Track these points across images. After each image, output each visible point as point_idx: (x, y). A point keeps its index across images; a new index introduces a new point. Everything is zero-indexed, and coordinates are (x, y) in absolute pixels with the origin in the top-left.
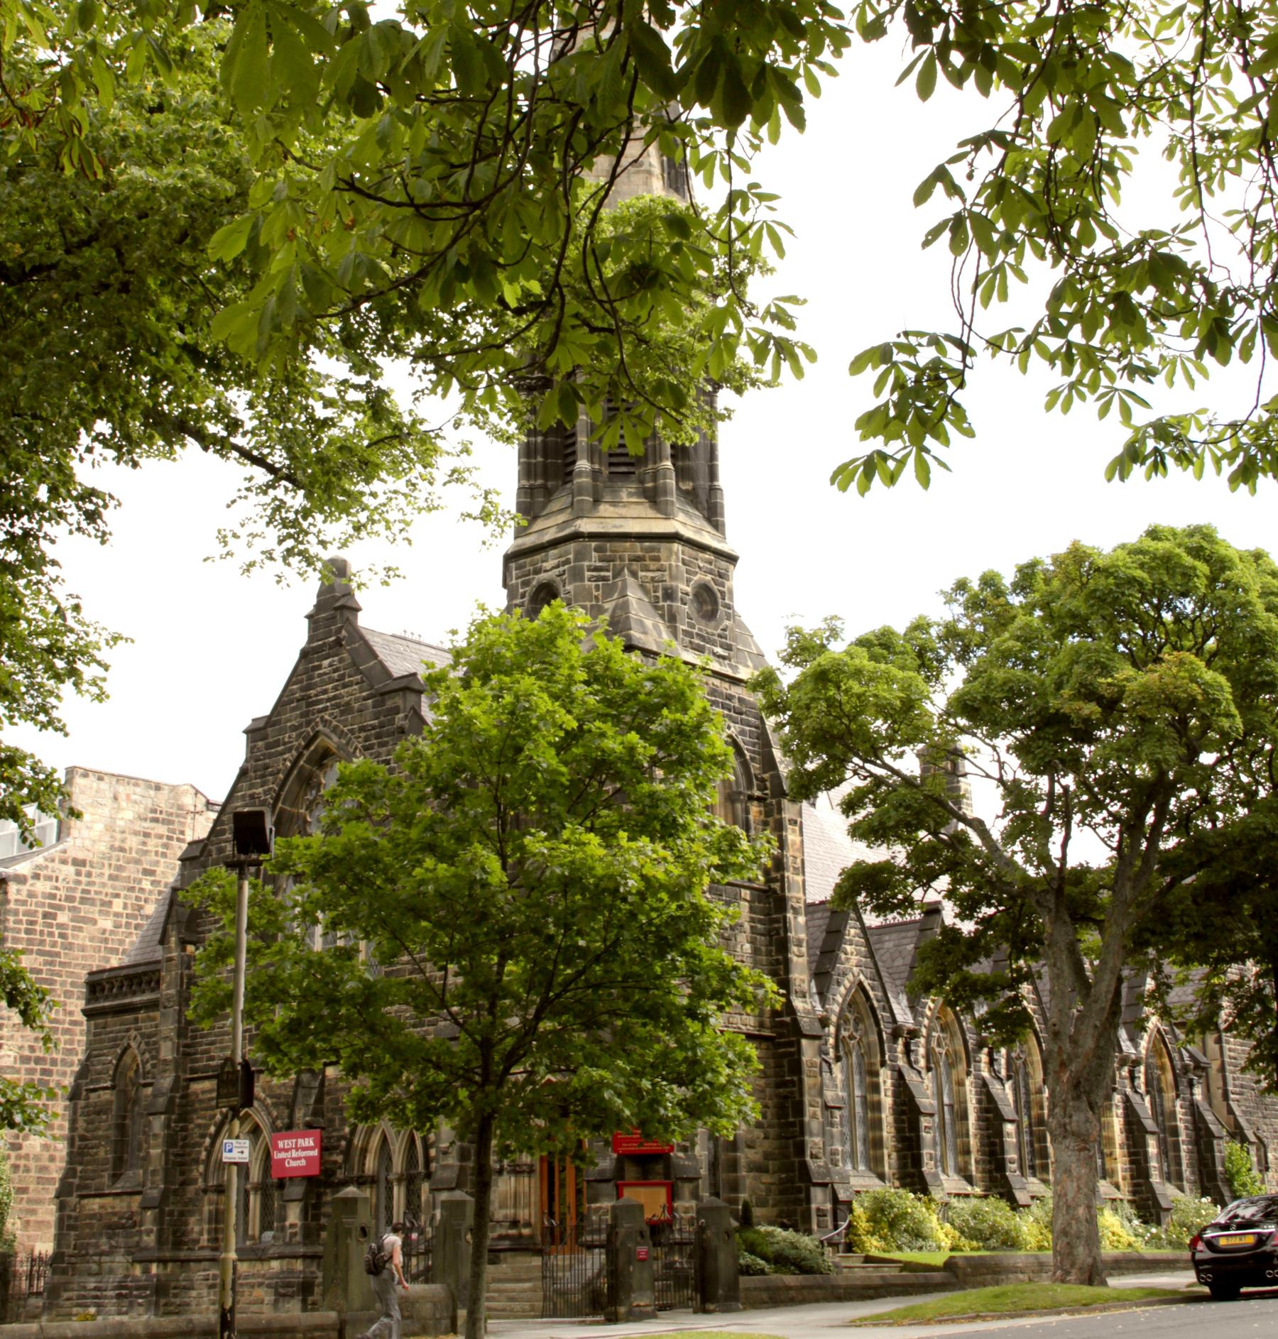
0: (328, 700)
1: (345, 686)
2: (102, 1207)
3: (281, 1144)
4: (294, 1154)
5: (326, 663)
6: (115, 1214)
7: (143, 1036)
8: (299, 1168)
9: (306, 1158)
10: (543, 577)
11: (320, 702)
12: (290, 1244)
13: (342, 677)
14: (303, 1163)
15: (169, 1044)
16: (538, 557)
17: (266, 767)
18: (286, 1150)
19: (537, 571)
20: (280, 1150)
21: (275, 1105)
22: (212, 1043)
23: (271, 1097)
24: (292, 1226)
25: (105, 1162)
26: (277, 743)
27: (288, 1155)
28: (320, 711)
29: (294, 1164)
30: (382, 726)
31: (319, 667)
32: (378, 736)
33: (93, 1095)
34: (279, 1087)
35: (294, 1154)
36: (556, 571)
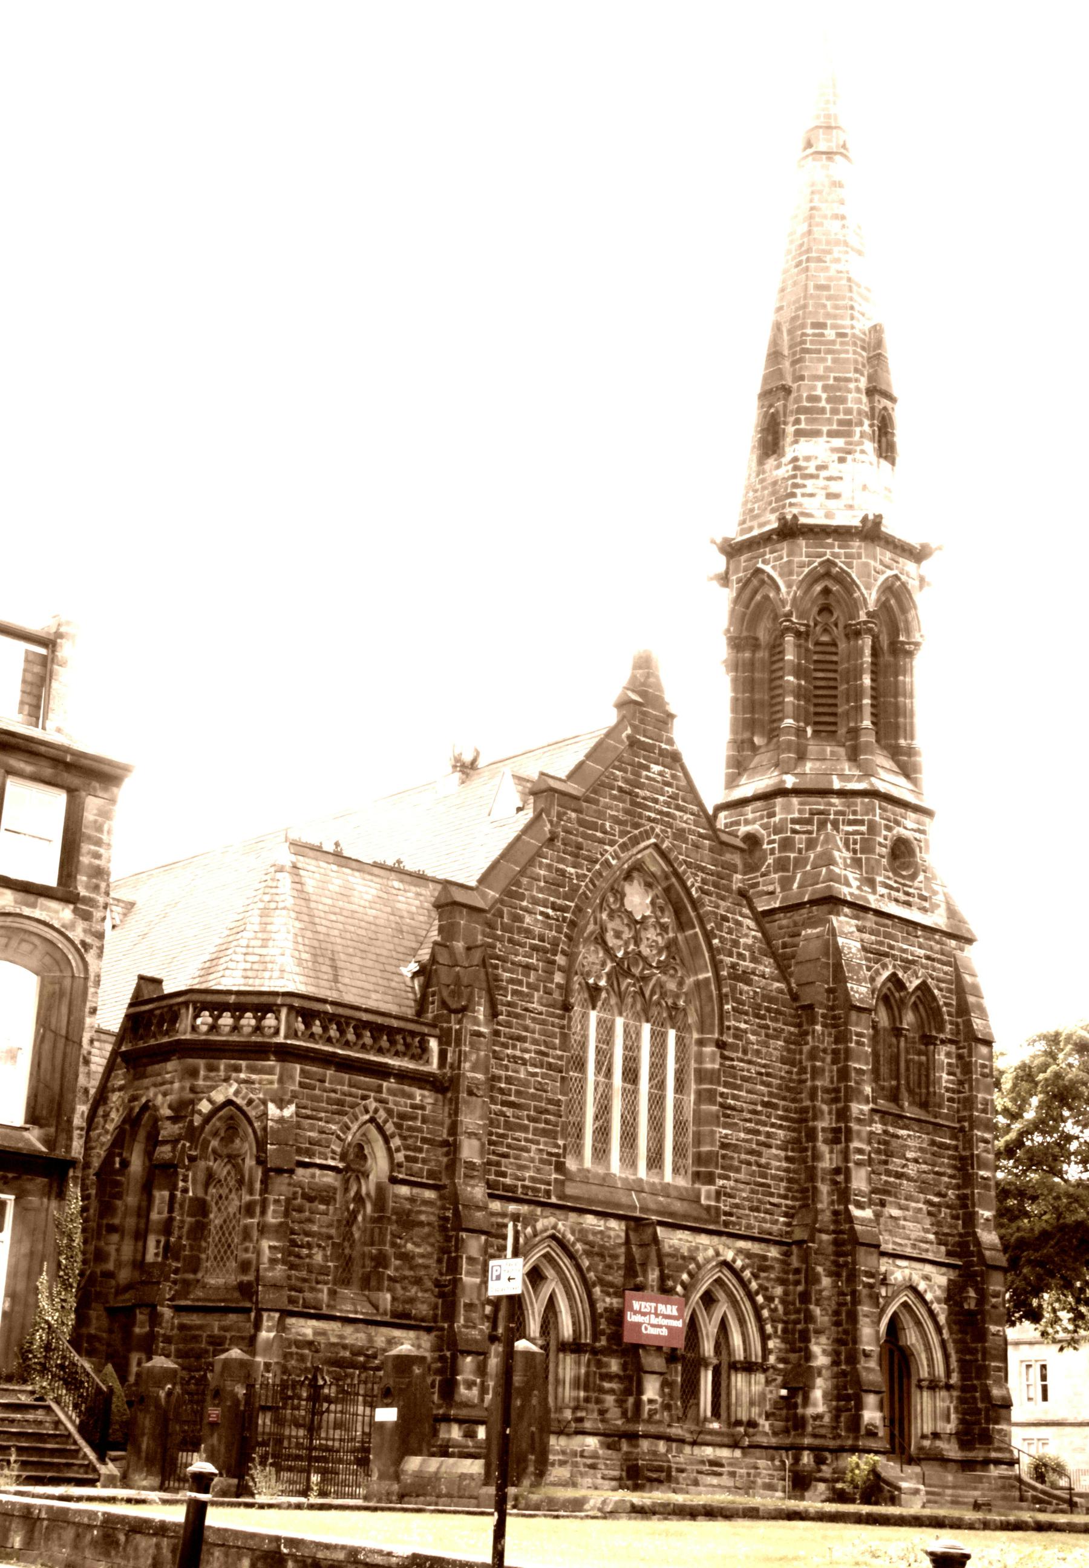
0: (660, 813)
1: (678, 808)
2: (316, 1333)
3: (636, 1305)
4: (654, 1320)
5: (656, 768)
6: (345, 1347)
7: (390, 1112)
8: (658, 1337)
9: (668, 1327)
10: (898, 831)
11: (649, 809)
12: (649, 1421)
13: (674, 797)
14: (664, 1332)
15: (475, 1143)
16: (899, 810)
17: (579, 847)
18: (644, 1314)
19: (898, 823)
20: (636, 1313)
21: (588, 1254)
22: (506, 1156)
23: (586, 1243)
24: (651, 1401)
25: (324, 1271)
26: (594, 827)
27: (646, 1319)
28: (649, 819)
29: (652, 1331)
30: (719, 876)
31: (648, 769)
32: (716, 885)
33: (300, 1171)
34: (595, 1233)
35: (654, 1320)
36: (918, 835)
